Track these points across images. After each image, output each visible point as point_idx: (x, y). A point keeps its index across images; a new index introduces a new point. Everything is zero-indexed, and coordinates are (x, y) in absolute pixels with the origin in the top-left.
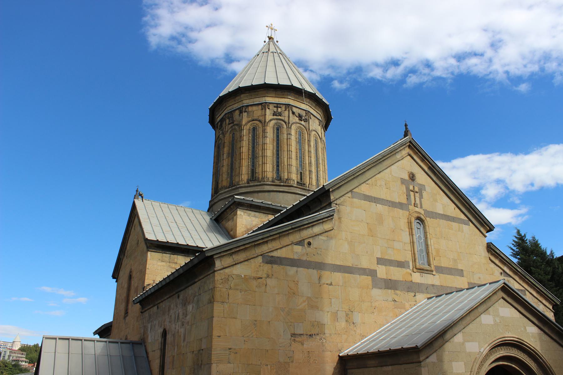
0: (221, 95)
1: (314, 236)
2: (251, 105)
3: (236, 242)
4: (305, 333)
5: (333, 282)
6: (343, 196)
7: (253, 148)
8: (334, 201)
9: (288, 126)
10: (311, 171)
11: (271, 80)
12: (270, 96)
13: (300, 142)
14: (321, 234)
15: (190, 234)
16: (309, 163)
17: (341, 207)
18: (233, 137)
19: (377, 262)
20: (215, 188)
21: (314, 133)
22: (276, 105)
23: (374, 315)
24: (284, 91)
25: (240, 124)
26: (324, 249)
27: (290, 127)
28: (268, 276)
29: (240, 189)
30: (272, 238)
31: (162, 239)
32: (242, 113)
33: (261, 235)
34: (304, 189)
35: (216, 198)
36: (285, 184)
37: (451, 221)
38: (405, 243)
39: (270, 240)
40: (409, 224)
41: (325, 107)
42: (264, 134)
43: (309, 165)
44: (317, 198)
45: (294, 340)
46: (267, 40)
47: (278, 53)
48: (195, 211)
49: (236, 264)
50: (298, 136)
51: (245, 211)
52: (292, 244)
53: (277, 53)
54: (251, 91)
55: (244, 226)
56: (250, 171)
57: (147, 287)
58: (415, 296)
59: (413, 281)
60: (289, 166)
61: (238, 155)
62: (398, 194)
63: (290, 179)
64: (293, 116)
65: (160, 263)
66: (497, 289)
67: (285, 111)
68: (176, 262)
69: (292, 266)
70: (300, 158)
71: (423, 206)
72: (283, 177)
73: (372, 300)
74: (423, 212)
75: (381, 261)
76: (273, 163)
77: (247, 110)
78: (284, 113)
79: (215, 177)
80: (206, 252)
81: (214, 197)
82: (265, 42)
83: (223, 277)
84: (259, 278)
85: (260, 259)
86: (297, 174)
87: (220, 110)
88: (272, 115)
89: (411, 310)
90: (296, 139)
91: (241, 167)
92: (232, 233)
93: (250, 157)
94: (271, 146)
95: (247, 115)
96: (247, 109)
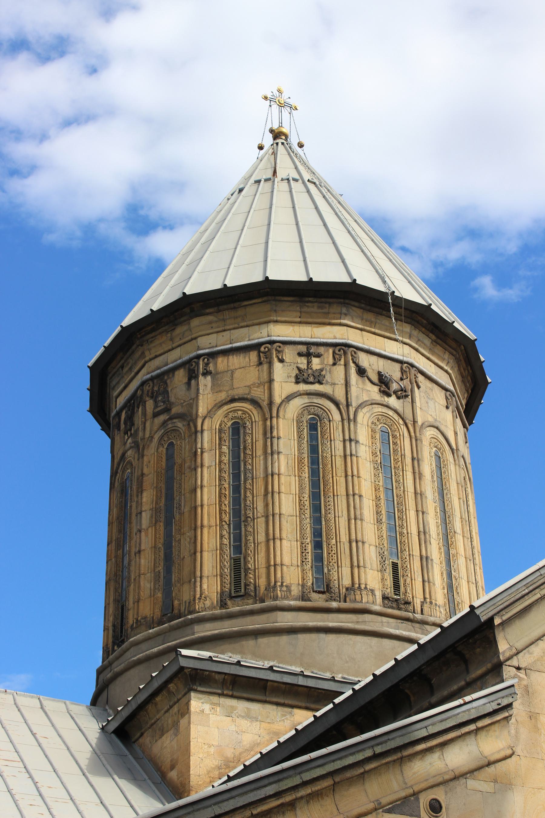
0: (126, 322)
1: (451, 780)
2: (225, 353)
3: (190, 809)
7: (236, 489)
9: (345, 416)
10: (427, 558)
12: (283, 319)
14: (472, 772)
15: (35, 783)
16: (419, 532)
17: (534, 676)
18: (170, 457)
20: (114, 626)
21: (430, 432)
22: (303, 349)
24: (330, 303)
25: (191, 415)
27: (352, 417)
29: (197, 628)
30: (308, 790)
32: (196, 377)
33: (270, 784)
34: (408, 620)
35: (117, 658)
36: (343, 605)
39: (302, 798)
41: (463, 347)
42: (269, 444)
44: (453, 648)
46: (268, 140)
47: (304, 182)
48: (50, 704)
50: (378, 444)
51: (215, 699)
52: (376, 809)
53: (300, 181)
54: (221, 308)
55: (212, 750)
56: (227, 565)
60: (354, 544)
61: (186, 515)
63: (359, 587)
64: (360, 382)
67: (335, 367)
70: (389, 518)
72: (336, 582)
76: (303, 537)
77: (211, 367)
78: (330, 372)
79: (116, 590)
81: (111, 657)
86: (382, 570)
87: (125, 370)
88: (294, 380)
90: (374, 454)
91: (198, 555)
92: (173, 775)
93: (227, 519)
95: (213, 385)
96: (211, 365)
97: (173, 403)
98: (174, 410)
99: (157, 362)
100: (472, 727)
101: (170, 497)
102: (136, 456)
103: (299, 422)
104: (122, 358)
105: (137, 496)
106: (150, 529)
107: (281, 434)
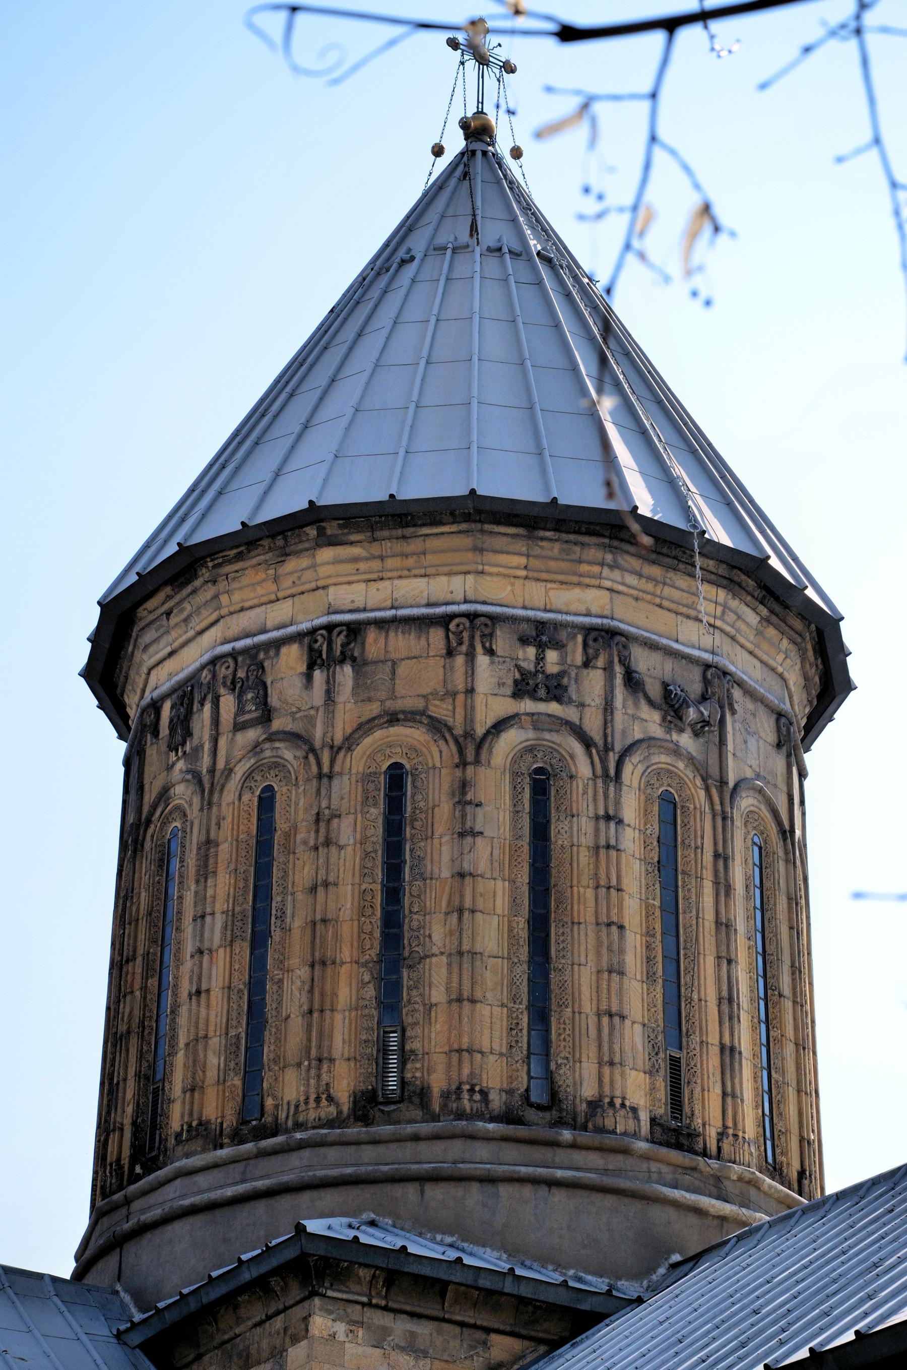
2: (381, 624)
10: (732, 1049)
16: (720, 999)
27: (612, 772)
41: (813, 627)
46: (455, 143)
61: (296, 934)
63: (612, 1104)
64: (630, 703)
67: (585, 672)
78: (576, 681)
82: (438, 151)
86: (651, 1072)
87: (174, 620)
88: (509, 691)
94: (501, 888)
95: (356, 686)
97: (276, 710)
98: (277, 724)
102: (196, 800)
103: (515, 774)
104: (169, 597)
105: (197, 881)
106: (221, 951)
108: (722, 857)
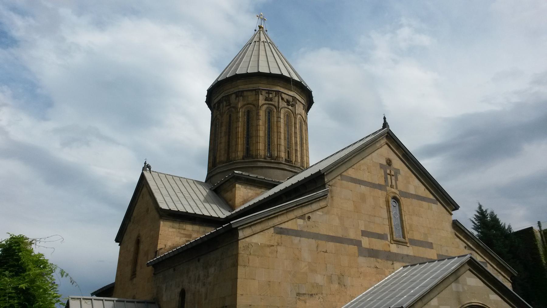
3: (254, 217)
4: (307, 293)
5: (327, 250)
6: (334, 178)
8: (327, 183)
9: (278, 111)
10: (297, 150)
11: (264, 69)
13: (288, 125)
14: (317, 210)
15: (196, 203)
17: (333, 187)
19: (362, 234)
21: (299, 116)
22: (267, 91)
23: (360, 279)
26: (320, 223)
27: (279, 111)
28: (278, 244)
30: (281, 213)
31: (173, 208)
37: (421, 200)
38: (384, 219)
40: (387, 202)
43: (295, 145)
45: (299, 298)
46: (258, 29)
47: (268, 43)
49: (254, 234)
52: (296, 218)
57: (159, 251)
58: (393, 264)
59: (391, 251)
62: (377, 176)
65: (171, 230)
66: (465, 262)
68: (185, 228)
69: (296, 236)
70: (288, 139)
71: (398, 187)
73: (358, 266)
74: (398, 193)
75: (365, 233)
78: (274, 98)
80: (232, 225)
81: (212, 170)
83: (244, 245)
84: (272, 246)
85: (272, 230)
86: (285, 153)
89: (390, 276)
90: (284, 121)
92: (230, 203)
94: (264, 128)
98: (232, 105)
99: (227, 92)
100: (318, 199)
101: (230, 129)
103: (265, 111)
107: (261, 115)
108: (295, 123)
